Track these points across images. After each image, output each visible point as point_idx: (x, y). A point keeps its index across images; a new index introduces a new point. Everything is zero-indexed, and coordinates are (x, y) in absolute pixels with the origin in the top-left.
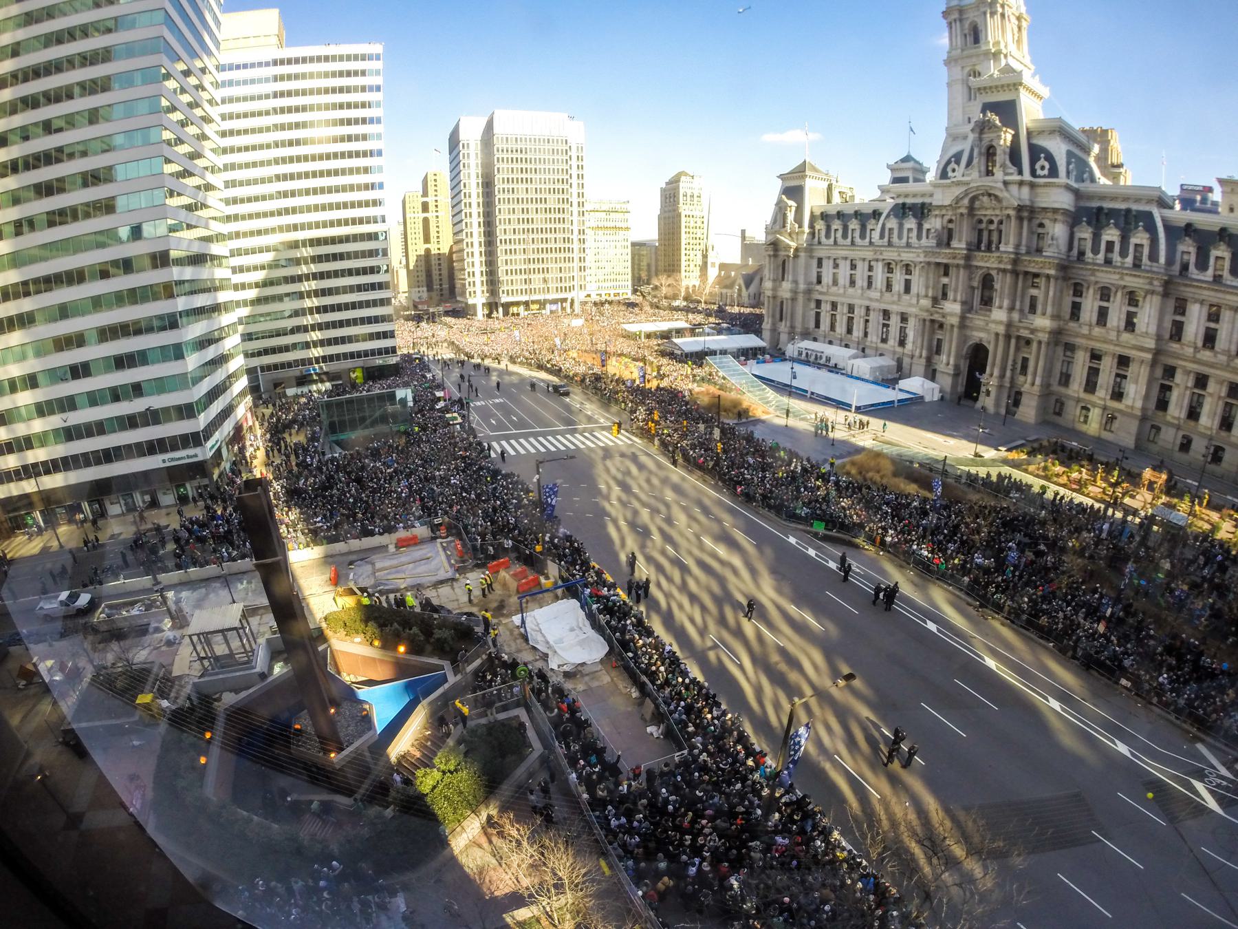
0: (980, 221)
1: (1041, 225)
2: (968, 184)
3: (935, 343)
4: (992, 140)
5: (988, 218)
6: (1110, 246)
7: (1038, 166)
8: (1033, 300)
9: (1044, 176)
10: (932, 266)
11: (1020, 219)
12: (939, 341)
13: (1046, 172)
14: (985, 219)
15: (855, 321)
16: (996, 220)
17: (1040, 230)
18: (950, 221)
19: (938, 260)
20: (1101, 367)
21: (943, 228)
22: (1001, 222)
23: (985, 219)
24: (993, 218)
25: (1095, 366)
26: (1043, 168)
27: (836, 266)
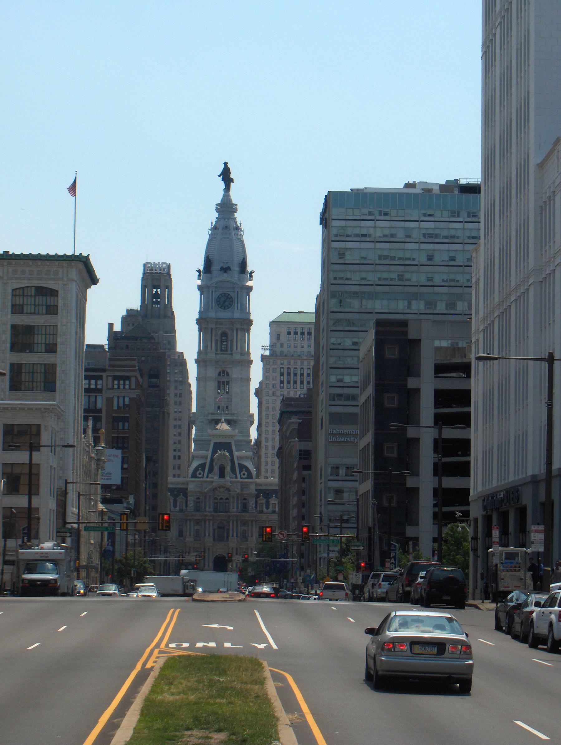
0: (216, 499)
1: (245, 499)
2: (212, 482)
5: (220, 497)
7: (242, 474)
9: (245, 478)
10: (192, 522)
11: (238, 498)
14: (219, 498)
17: (245, 501)
18: (198, 498)
23: (219, 498)
24: (223, 497)
26: (244, 474)
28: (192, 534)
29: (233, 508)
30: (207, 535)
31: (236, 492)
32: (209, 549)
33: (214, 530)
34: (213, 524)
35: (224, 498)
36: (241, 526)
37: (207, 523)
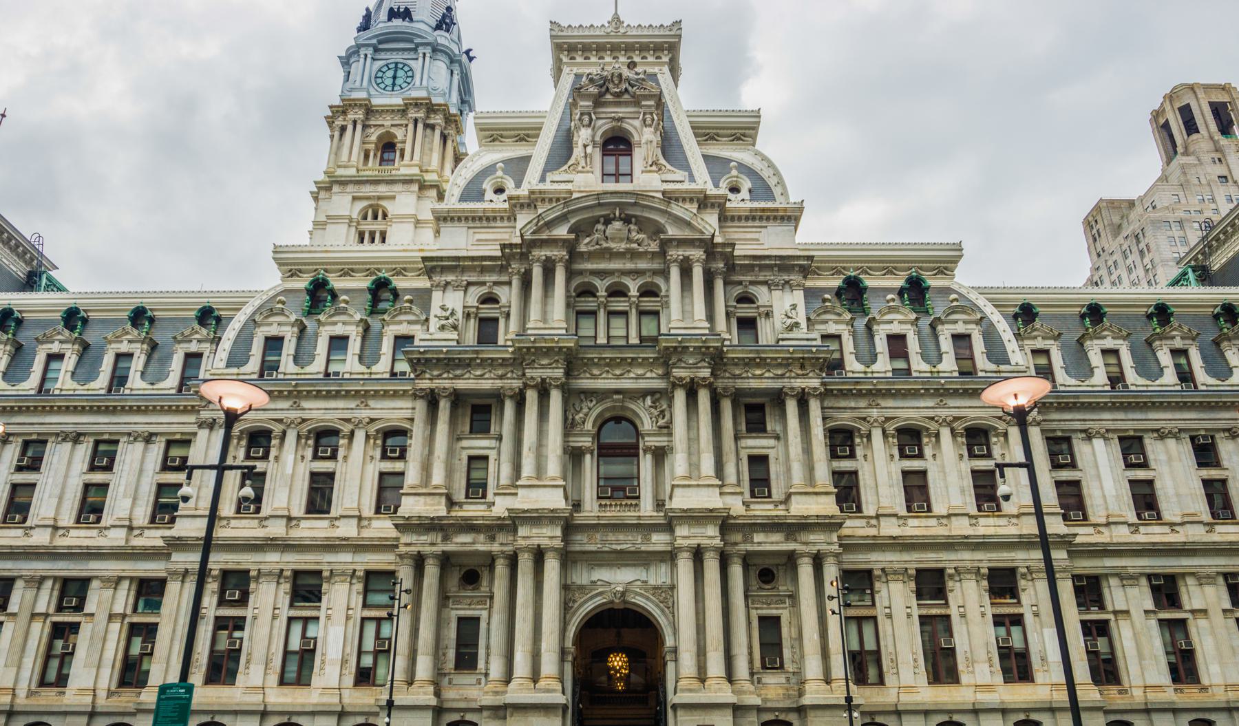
0: (589, 291)
1: (746, 299)
3: (451, 633)
4: (620, 119)
5: (608, 282)
6: (897, 344)
8: (759, 462)
12: (468, 627)
13: (744, 194)
14: (601, 286)
15: (83, 641)
16: (633, 287)
18: (490, 299)
19: (461, 385)
20: (954, 611)
21: (468, 316)
22: (649, 291)
23: (601, 286)
25: (934, 611)
27: (34, 465)
28: (438, 477)
29: (686, 313)
30: (528, 468)
31: (702, 233)
32: (539, 556)
33: (574, 456)
34: (569, 427)
35: (633, 287)
36: (737, 438)
37: (531, 397)
